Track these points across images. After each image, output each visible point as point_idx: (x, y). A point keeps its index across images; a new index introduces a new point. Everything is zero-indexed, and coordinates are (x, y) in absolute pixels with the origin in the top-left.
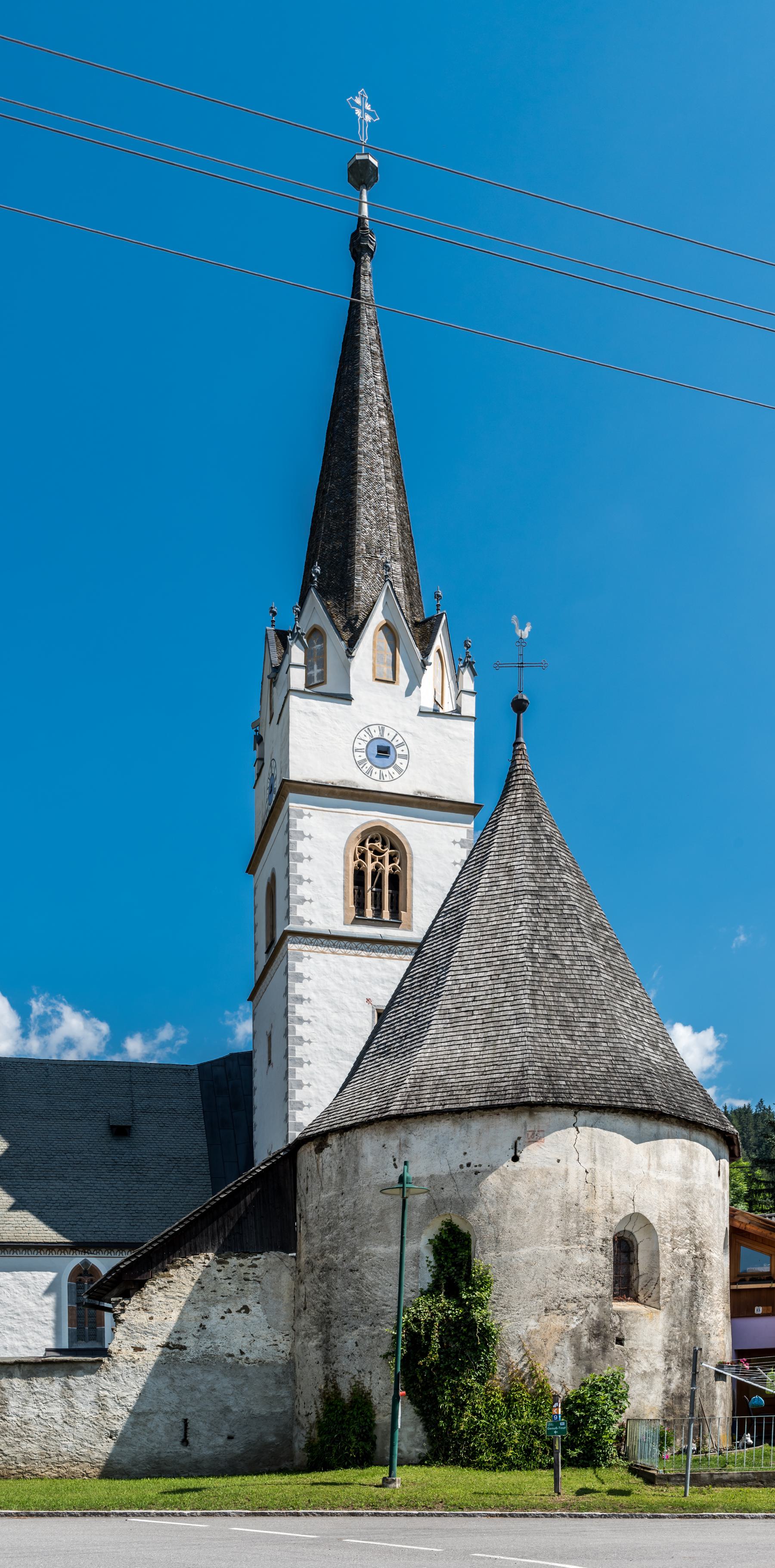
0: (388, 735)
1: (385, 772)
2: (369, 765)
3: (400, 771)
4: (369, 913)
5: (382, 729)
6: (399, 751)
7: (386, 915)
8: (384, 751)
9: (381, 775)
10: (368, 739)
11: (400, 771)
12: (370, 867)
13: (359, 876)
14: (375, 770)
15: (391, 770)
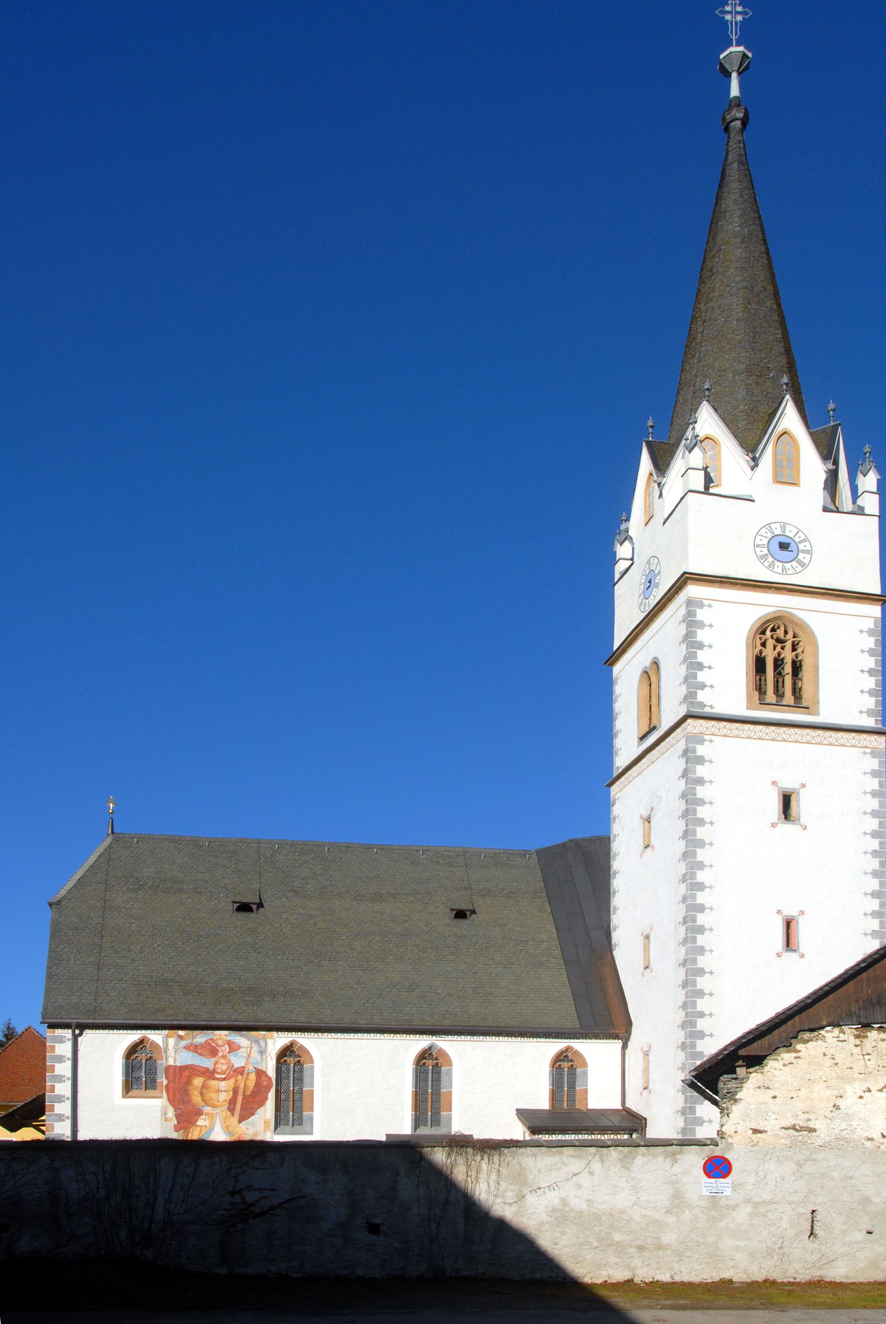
0: (790, 532)
1: (788, 565)
2: (770, 559)
3: (803, 565)
4: (771, 696)
5: (784, 528)
6: (801, 546)
7: (789, 698)
8: (784, 546)
9: (784, 569)
10: (770, 535)
11: (803, 565)
12: (770, 655)
13: (760, 664)
14: (777, 563)
15: (794, 564)
